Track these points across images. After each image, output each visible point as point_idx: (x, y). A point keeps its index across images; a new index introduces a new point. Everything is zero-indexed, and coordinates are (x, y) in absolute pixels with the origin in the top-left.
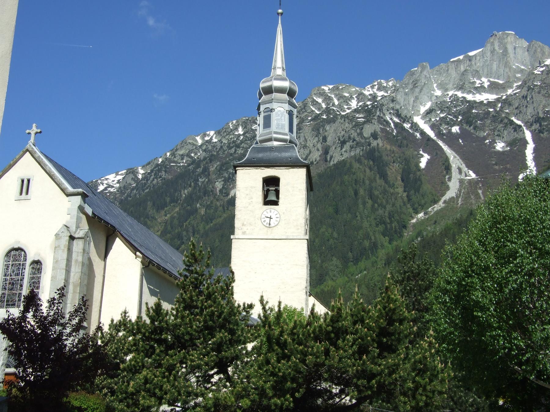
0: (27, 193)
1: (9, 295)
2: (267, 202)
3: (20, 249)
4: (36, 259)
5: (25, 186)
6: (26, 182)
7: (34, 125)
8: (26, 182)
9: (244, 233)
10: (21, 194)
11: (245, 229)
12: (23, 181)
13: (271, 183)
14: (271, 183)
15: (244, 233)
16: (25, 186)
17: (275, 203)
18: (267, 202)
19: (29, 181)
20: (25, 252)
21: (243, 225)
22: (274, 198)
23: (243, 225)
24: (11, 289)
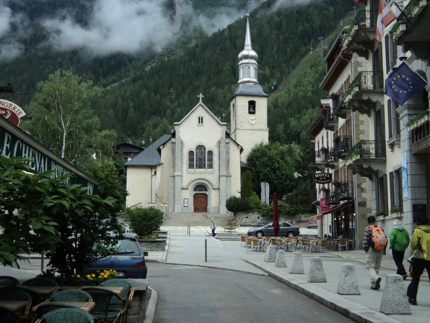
0: (202, 123)
1: (199, 164)
2: (250, 113)
3: (202, 146)
4: (210, 150)
5: (201, 120)
6: (201, 118)
7: (201, 94)
8: (201, 118)
9: (241, 126)
10: (199, 123)
11: (241, 124)
12: (199, 118)
13: (252, 105)
14: (252, 105)
15: (241, 126)
16: (201, 120)
17: (253, 113)
18: (250, 113)
19: (202, 118)
20: (204, 147)
21: (241, 123)
22: (252, 111)
23: (241, 123)
24: (200, 161)
